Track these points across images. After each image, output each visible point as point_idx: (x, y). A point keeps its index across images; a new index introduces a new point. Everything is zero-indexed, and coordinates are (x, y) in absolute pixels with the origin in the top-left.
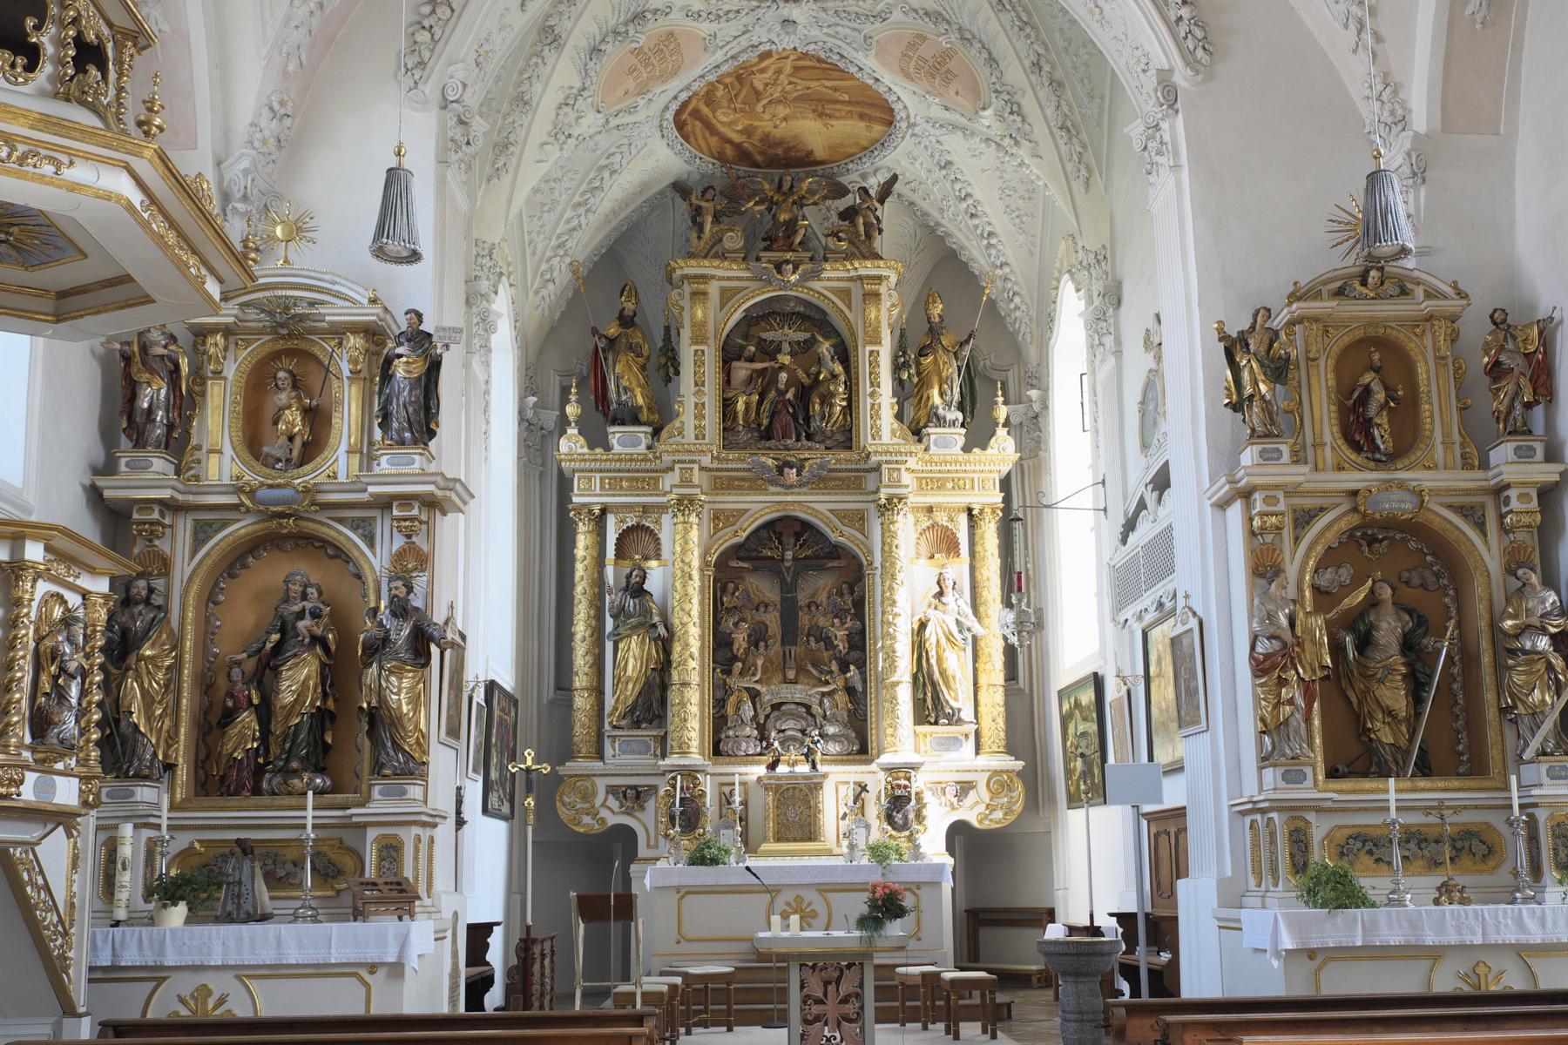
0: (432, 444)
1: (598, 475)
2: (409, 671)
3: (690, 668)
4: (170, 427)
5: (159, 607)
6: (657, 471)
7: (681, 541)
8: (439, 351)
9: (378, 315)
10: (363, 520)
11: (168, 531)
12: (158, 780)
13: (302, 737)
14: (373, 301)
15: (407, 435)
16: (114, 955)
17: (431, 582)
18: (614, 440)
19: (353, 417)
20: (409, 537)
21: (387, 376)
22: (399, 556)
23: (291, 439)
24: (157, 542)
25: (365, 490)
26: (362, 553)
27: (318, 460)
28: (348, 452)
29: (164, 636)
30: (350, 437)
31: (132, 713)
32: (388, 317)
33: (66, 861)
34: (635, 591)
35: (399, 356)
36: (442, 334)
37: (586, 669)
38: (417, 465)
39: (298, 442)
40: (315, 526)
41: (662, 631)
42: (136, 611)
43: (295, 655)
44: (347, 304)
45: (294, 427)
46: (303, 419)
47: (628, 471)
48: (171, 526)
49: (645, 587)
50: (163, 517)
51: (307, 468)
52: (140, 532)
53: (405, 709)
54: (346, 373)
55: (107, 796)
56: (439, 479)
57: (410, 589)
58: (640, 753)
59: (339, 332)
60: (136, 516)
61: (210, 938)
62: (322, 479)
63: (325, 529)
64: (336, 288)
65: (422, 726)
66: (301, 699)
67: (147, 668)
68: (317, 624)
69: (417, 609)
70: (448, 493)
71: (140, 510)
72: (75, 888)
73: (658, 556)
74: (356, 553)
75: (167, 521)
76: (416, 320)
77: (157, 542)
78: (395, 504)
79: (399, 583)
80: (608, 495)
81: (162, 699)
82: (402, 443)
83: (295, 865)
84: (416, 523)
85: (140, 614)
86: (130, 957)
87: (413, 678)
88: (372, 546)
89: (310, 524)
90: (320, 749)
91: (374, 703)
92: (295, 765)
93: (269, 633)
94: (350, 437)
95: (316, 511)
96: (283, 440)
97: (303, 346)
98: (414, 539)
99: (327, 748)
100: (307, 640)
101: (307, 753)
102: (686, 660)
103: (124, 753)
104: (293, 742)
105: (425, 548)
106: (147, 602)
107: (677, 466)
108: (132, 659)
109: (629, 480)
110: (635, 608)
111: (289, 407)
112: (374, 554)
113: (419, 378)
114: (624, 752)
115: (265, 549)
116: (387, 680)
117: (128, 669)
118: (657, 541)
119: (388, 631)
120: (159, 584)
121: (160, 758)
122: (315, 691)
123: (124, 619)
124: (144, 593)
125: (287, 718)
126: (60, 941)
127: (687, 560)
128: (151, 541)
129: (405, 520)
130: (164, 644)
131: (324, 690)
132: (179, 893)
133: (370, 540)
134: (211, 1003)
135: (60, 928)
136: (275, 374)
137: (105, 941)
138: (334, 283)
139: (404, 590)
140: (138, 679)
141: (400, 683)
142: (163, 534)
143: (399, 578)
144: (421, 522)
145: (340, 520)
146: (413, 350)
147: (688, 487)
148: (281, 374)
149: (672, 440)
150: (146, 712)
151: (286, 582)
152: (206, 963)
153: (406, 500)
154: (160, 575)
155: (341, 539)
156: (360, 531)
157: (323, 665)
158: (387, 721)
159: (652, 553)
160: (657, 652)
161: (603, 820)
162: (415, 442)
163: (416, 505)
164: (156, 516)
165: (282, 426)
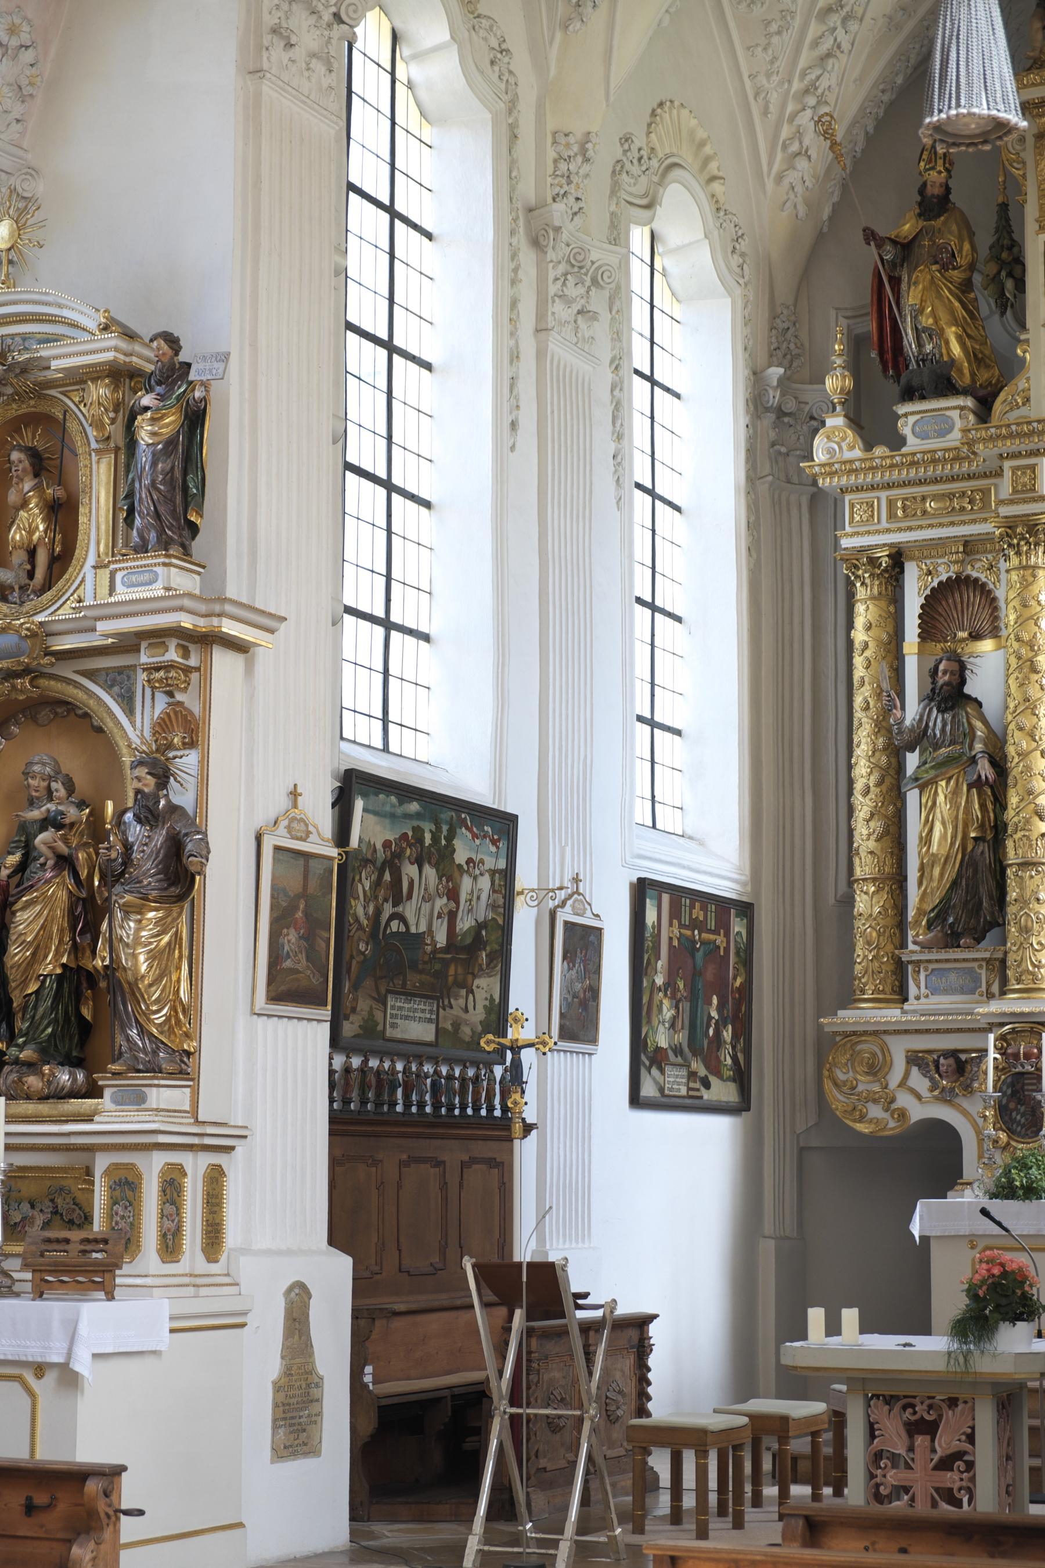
0: (197, 545)
1: (884, 495)
2: (156, 909)
3: (1035, 835)
6: (985, 476)
7: (1016, 603)
8: (198, 394)
9: (116, 349)
10: (120, 670)
13: (41, 1010)
14: (106, 328)
15: (152, 536)
17: (204, 763)
18: (906, 427)
19: (102, 512)
20: (170, 694)
21: (132, 444)
22: (162, 726)
23: (32, 553)
25: (94, 630)
26: (118, 723)
27: (60, 583)
28: (95, 567)
30: (98, 543)
32: (138, 348)
34: (945, 700)
35: (146, 409)
36: (201, 366)
37: (872, 844)
38: (159, 584)
39: (42, 558)
40: (59, 685)
41: (984, 769)
43: (32, 886)
44: (87, 337)
45: (31, 532)
46: (47, 519)
47: (936, 481)
49: (967, 690)
51: (48, 595)
53: (143, 968)
54: (94, 445)
56: (187, 603)
57: (163, 776)
58: (962, 991)
59: (79, 378)
62: (65, 612)
63: (71, 690)
64: (65, 313)
65: (184, 995)
66: (41, 953)
68: (65, 840)
69: (174, 809)
70: (215, 621)
73: (994, 632)
74: (111, 724)
76: (165, 347)
78: (144, 645)
79: (142, 771)
80: (900, 530)
82: (142, 548)
83: (33, 1207)
84: (172, 674)
87: (161, 919)
88: (130, 712)
89: (52, 683)
90: (74, 1029)
91: (107, 963)
92: (26, 1054)
93: (10, 853)
94: (98, 543)
95: (52, 665)
96: (19, 557)
97: (43, 408)
98: (179, 697)
99: (86, 1029)
100: (50, 863)
101: (52, 1035)
102: (1028, 821)
104: (33, 1017)
105: (196, 709)
107: (1007, 465)
109: (935, 498)
110: (943, 730)
111: (24, 504)
112: (134, 726)
113: (171, 444)
114: (934, 991)
115: (17, 723)
116: (122, 927)
118: (992, 602)
119: (132, 847)
122: (61, 941)
125: (25, 983)
127: (1026, 637)
129: (158, 669)
131: (73, 939)
133: (128, 703)
136: (9, 455)
138: (60, 306)
139: (151, 781)
141: (138, 930)
143: (141, 763)
144: (187, 670)
145: (90, 674)
146: (162, 398)
147: (1025, 501)
148: (15, 456)
149: (1013, 416)
151: (26, 774)
153: (158, 636)
155: (92, 702)
156: (116, 689)
157: (74, 901)
158: (126, 986)
159: (986, 626)
160: (983, 806)
161: (902, 1114)
162: (165, 544)
163: (173, 644)
165: (16, 535)
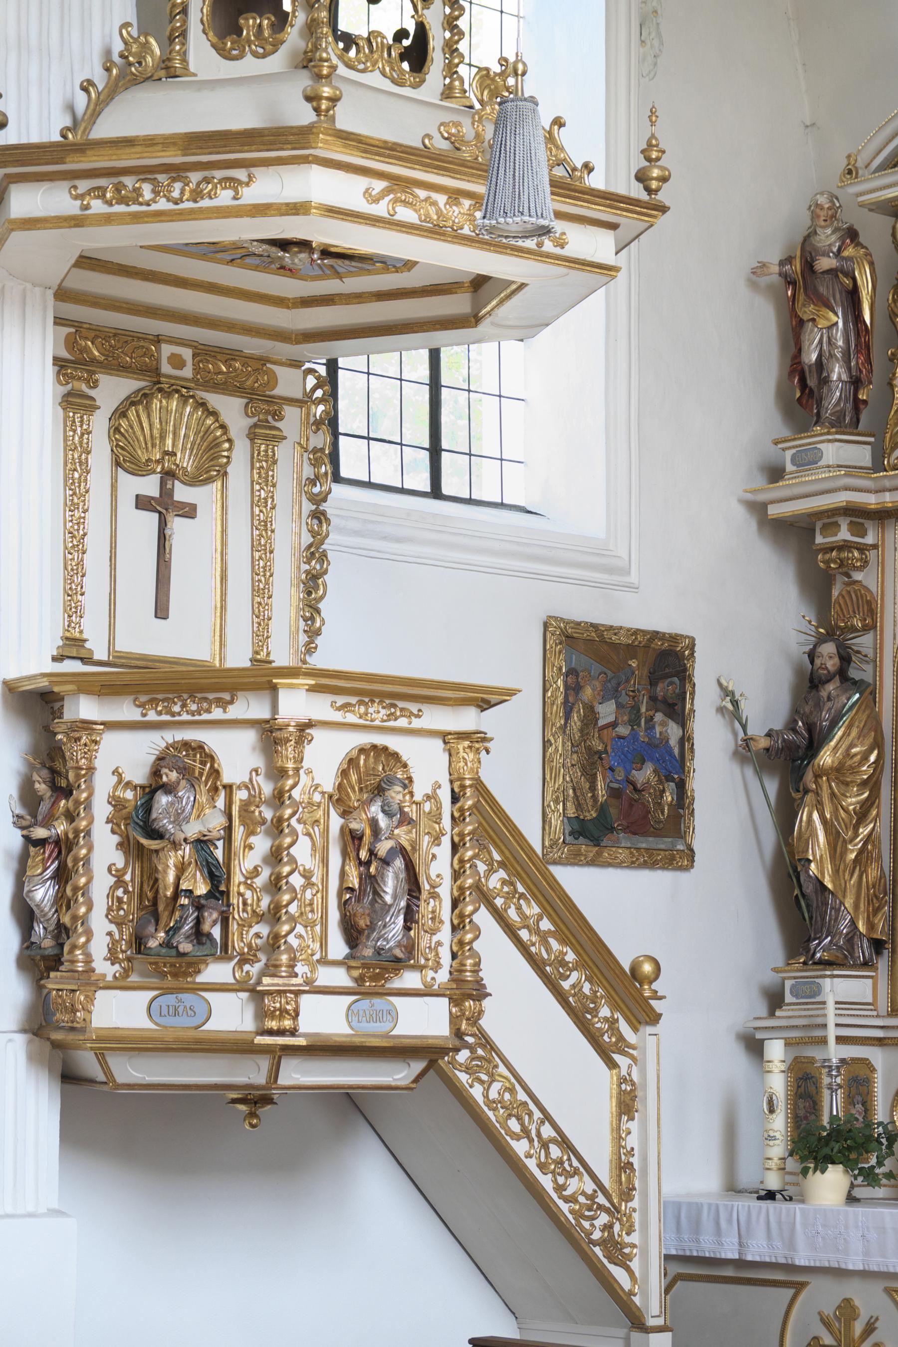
4: (856, 383)
5: (858, 685)
11: (872, 555)
12: (866, 964)
16: (741, 1244)
24: (858, 576)
29: (854, 732)
31: (809, 861)
33: (607, 1106)
42: (824, 694)
48: (875, 547)
50: (863, 535)
52: (827, 562)
55: (791, 993)
60: (819, 539)
61: (846, 1227)
67: (831, 787)
71: (825, 527)
72: (632, 1141)
75: (869, 539)
77: (858, 576)
81: (856, 835)
85: (829, 699)
86: (758, 1251)
103: (811, 924)
106: (842, 674)
108: (809, 776)
117: (806, 791)
120: (864, 642)
121: (861, 927)
123: (807, 709)
124: (832, 664)
126: (604, 1218)
128: (849, 576)
130: (852, 746)
132: (826, 1151)
134: (858, 1328)
135: (601, 1199)
137: (730, 1221)
140: (819, 805)
142: (866, 562)
150: (833, 858)
152: (843, 1266)
154: (866, 629)
164: (844, 534)
